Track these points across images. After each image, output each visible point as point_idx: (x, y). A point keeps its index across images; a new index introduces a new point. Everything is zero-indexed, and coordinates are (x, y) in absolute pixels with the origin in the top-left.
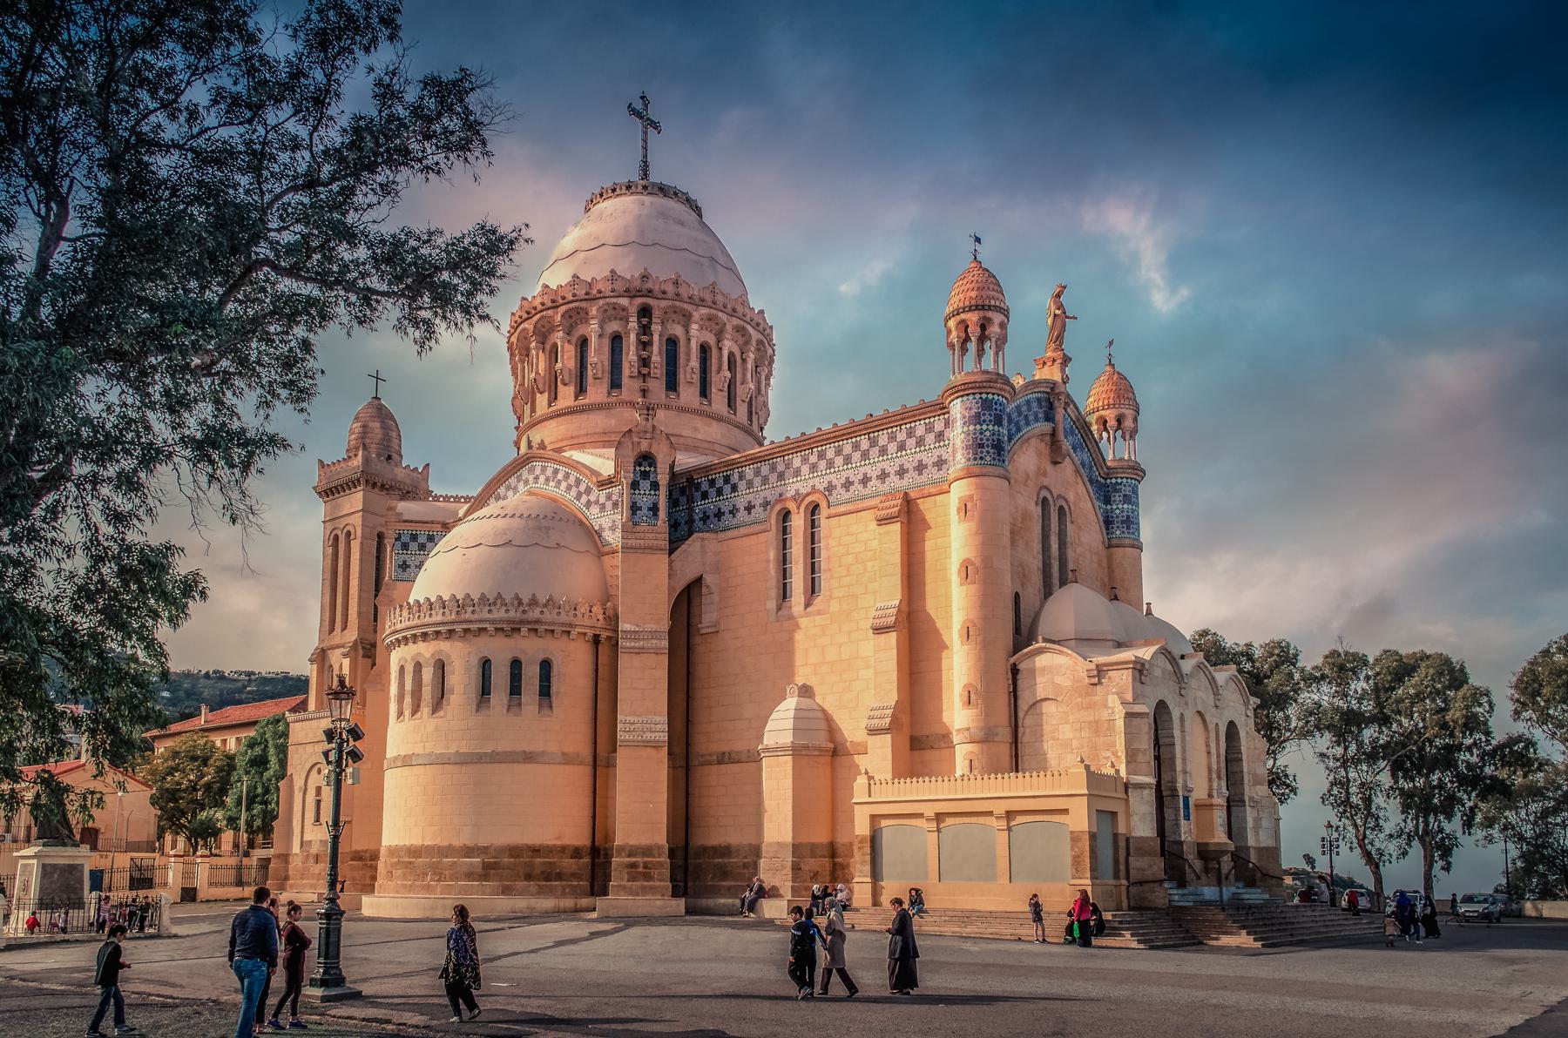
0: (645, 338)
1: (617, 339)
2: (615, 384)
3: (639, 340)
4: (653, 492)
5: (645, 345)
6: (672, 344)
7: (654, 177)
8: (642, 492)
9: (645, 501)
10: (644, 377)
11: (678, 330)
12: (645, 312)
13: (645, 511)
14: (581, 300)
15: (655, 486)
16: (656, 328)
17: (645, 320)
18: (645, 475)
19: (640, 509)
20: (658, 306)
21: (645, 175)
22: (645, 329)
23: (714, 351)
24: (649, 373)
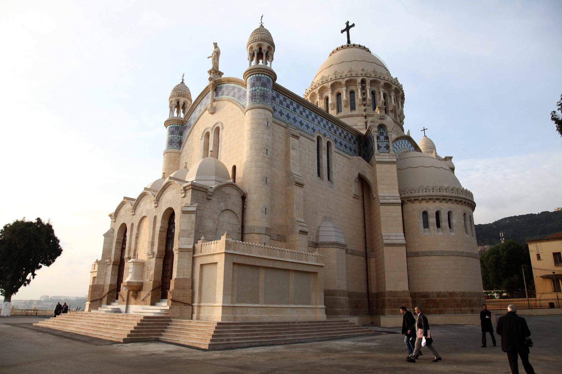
0: (364, 91)
1: (352, 93)
2: (353, 108)
3: (361, 92)
4: (385, 140)
5: (364, 94)
6: (373, 93)
7: (352, 43)
8: (381, 141)
9: (383, 145)
10: (365, 105)
11: (374, 89)
12: (363, 82)
13: (383, 148)
14: (339, 79)
15: (387, 138)
16: (368, 87)
17: (364, 85)
18: (382, 134)
19: (384, 147)
20: (368, 81)
21: (349, 42)
22: (363, 88)
23: (388, 97)
24: (366, 103)
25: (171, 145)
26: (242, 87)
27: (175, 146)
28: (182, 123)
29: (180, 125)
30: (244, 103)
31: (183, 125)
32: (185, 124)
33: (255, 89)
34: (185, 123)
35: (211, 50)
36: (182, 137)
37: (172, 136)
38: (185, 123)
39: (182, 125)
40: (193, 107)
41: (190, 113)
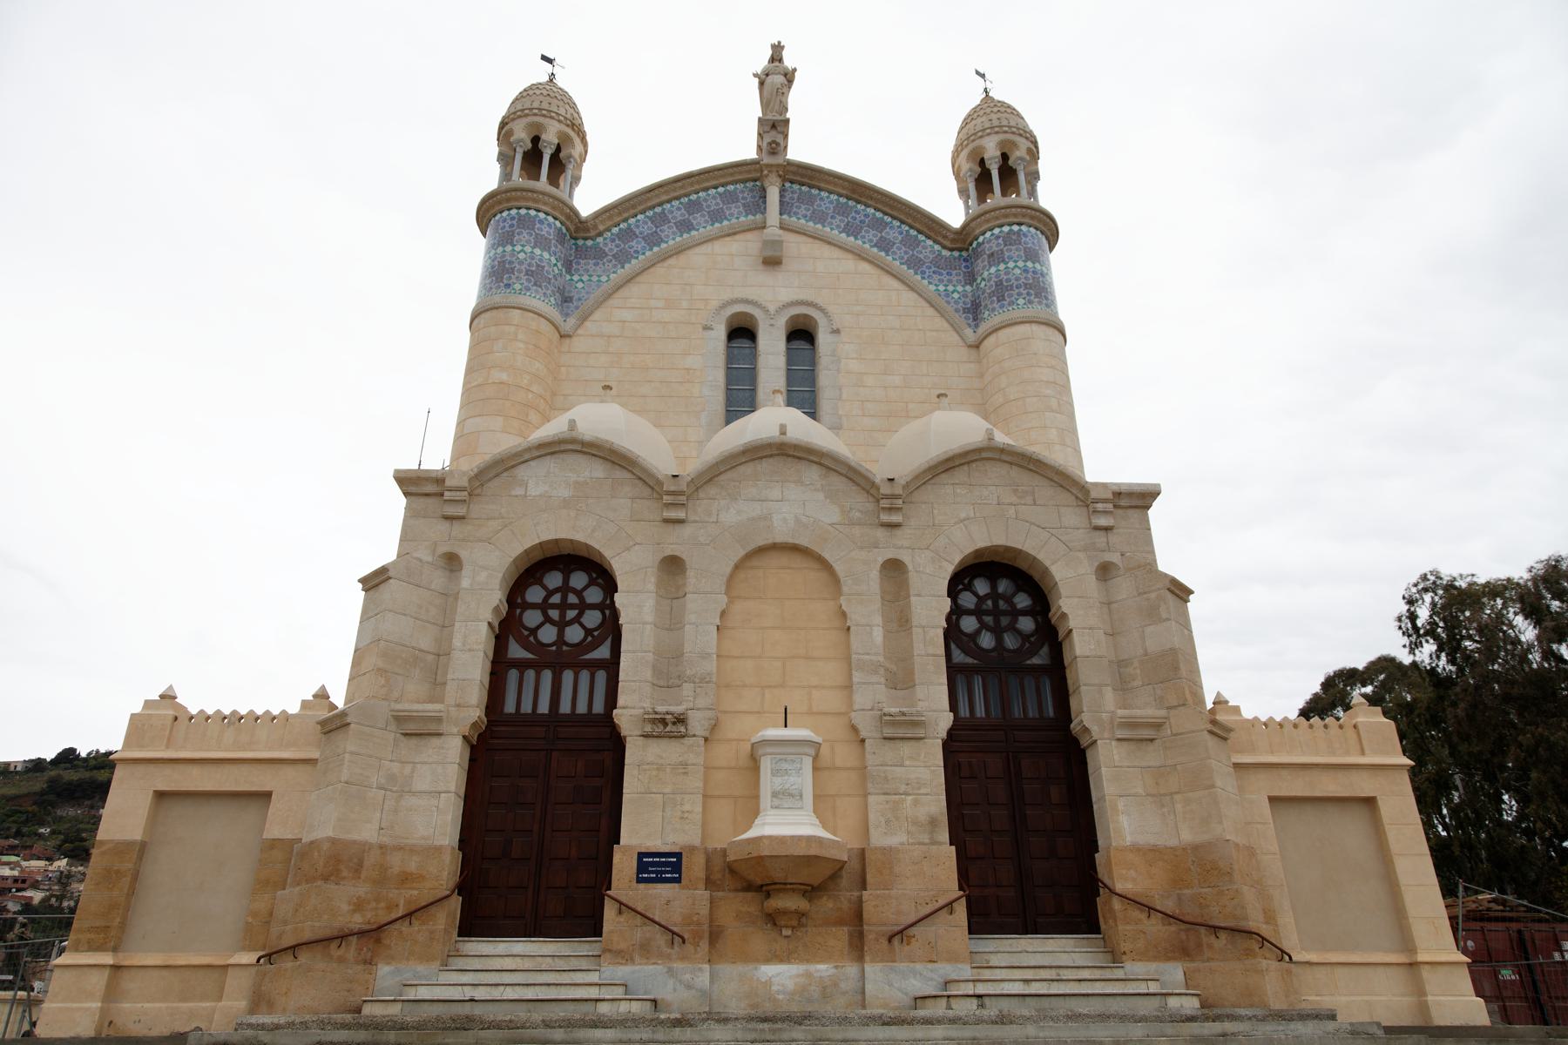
25: (540, 286)
26: (921, 237)
27: (552, 299)
28: (577, 230)
29: (568, 229)
30: (941, 288)
31: (576, 239)
32: (586, 239)
33: (1007, 268)
34: (592, 233)
35: (762, 61)
36: (568, 277)
37: (541, 255)
38: (592, 233)
39: (572, 237)
40: (649, 199)
41: (626, 210)
